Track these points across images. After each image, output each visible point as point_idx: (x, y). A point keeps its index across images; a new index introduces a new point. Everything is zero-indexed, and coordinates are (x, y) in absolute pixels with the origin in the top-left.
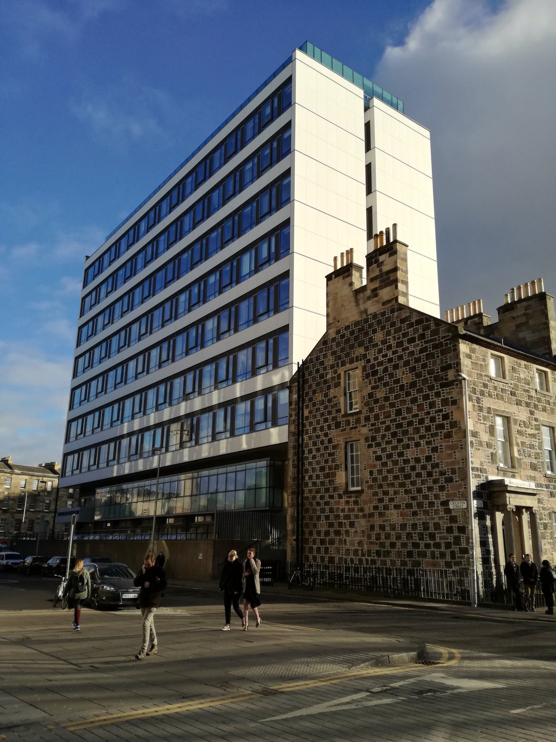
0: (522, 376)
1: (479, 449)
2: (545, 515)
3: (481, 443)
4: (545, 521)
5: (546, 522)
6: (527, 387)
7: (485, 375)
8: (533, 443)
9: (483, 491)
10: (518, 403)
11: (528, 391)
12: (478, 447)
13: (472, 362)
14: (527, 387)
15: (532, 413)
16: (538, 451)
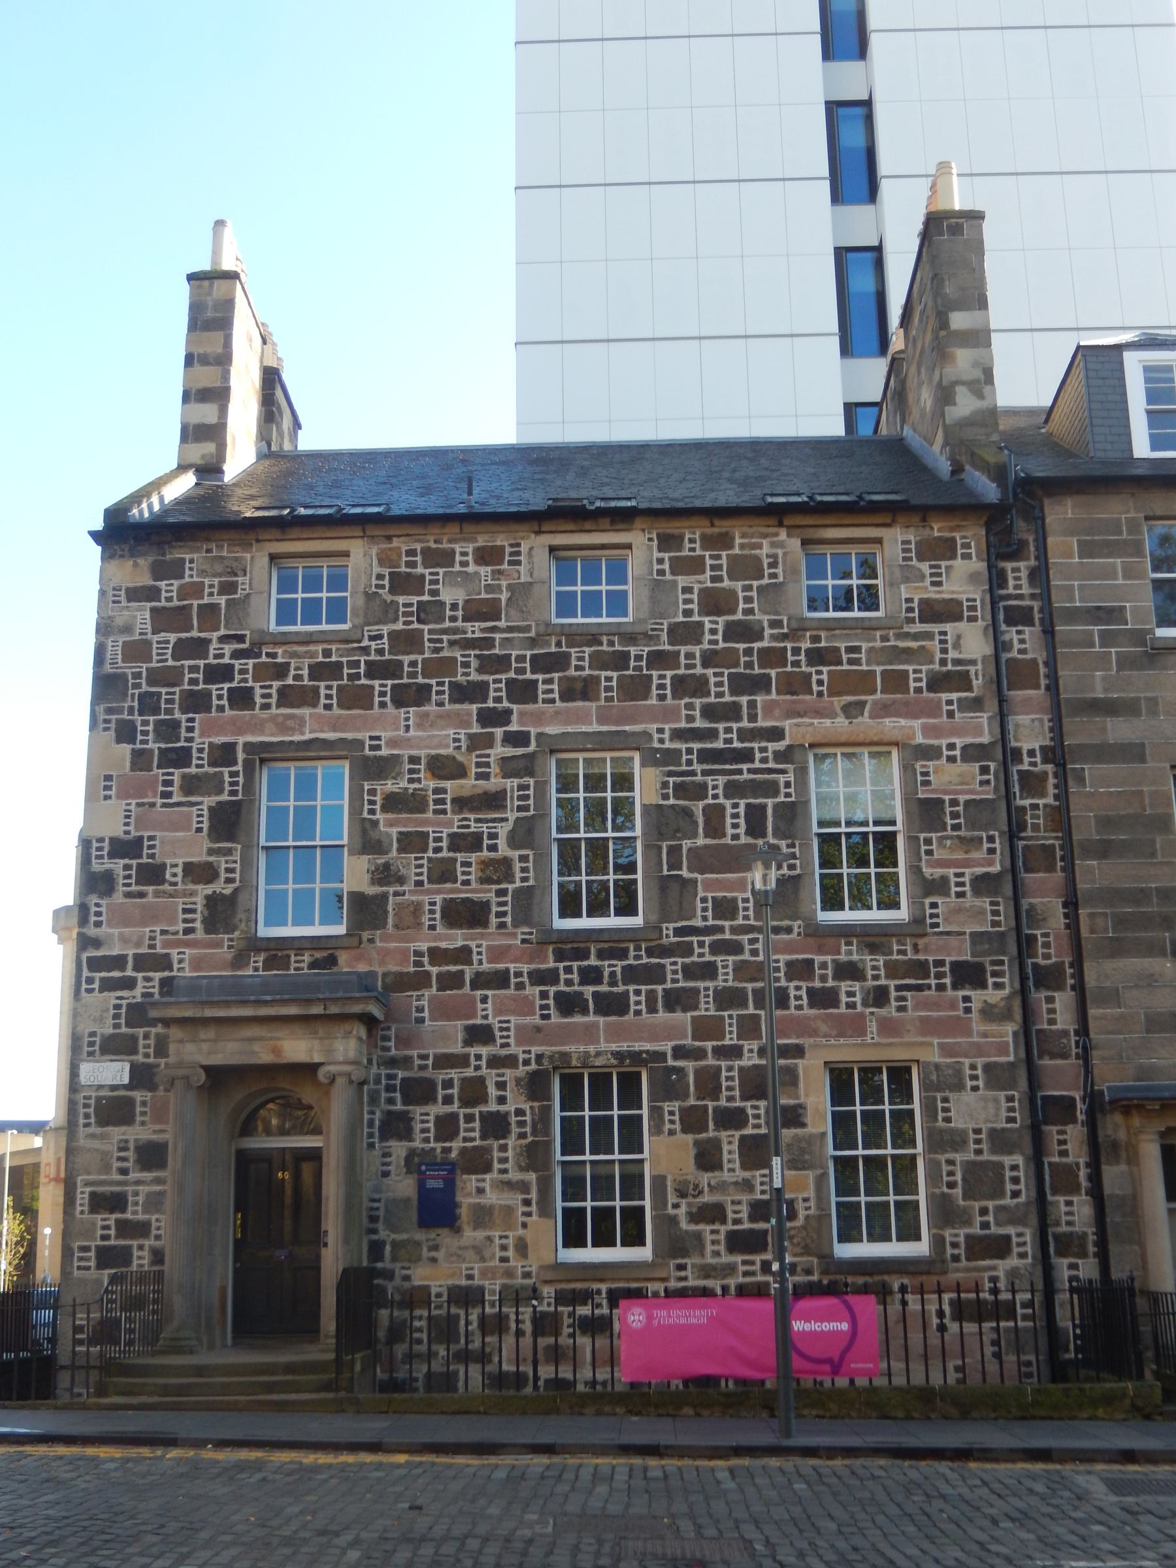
0: (448, 595)
1: (142, 895)
2: (501, 1086)
3: (153, 874)
4: (493, 1107)
5: (510, 1107)
6: (474, 630)
7: (223, 639)
8: (484, 828)
9: (141, 1031)
10: (410, 697)
11: (488, 643)
12: (134, 888)
13: (153, 610)
14: (474, 630)
15: (490, 718)
16: (504, 850)
